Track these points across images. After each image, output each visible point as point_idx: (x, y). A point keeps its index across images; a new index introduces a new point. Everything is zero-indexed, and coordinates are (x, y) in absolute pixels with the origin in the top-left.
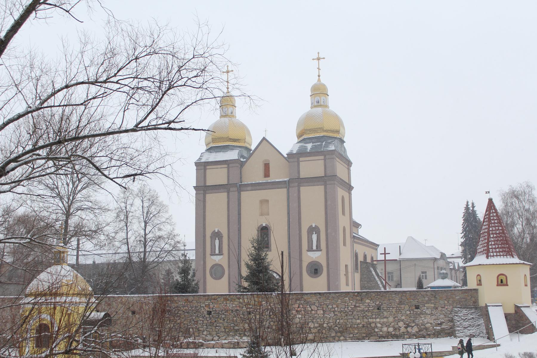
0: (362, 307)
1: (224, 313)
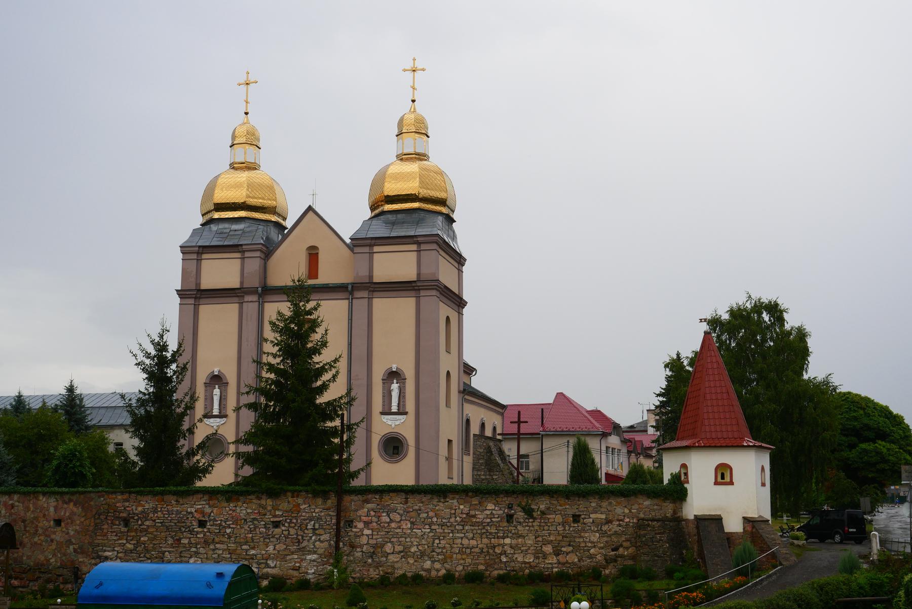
0: (480, 516)
1: (230, 524)
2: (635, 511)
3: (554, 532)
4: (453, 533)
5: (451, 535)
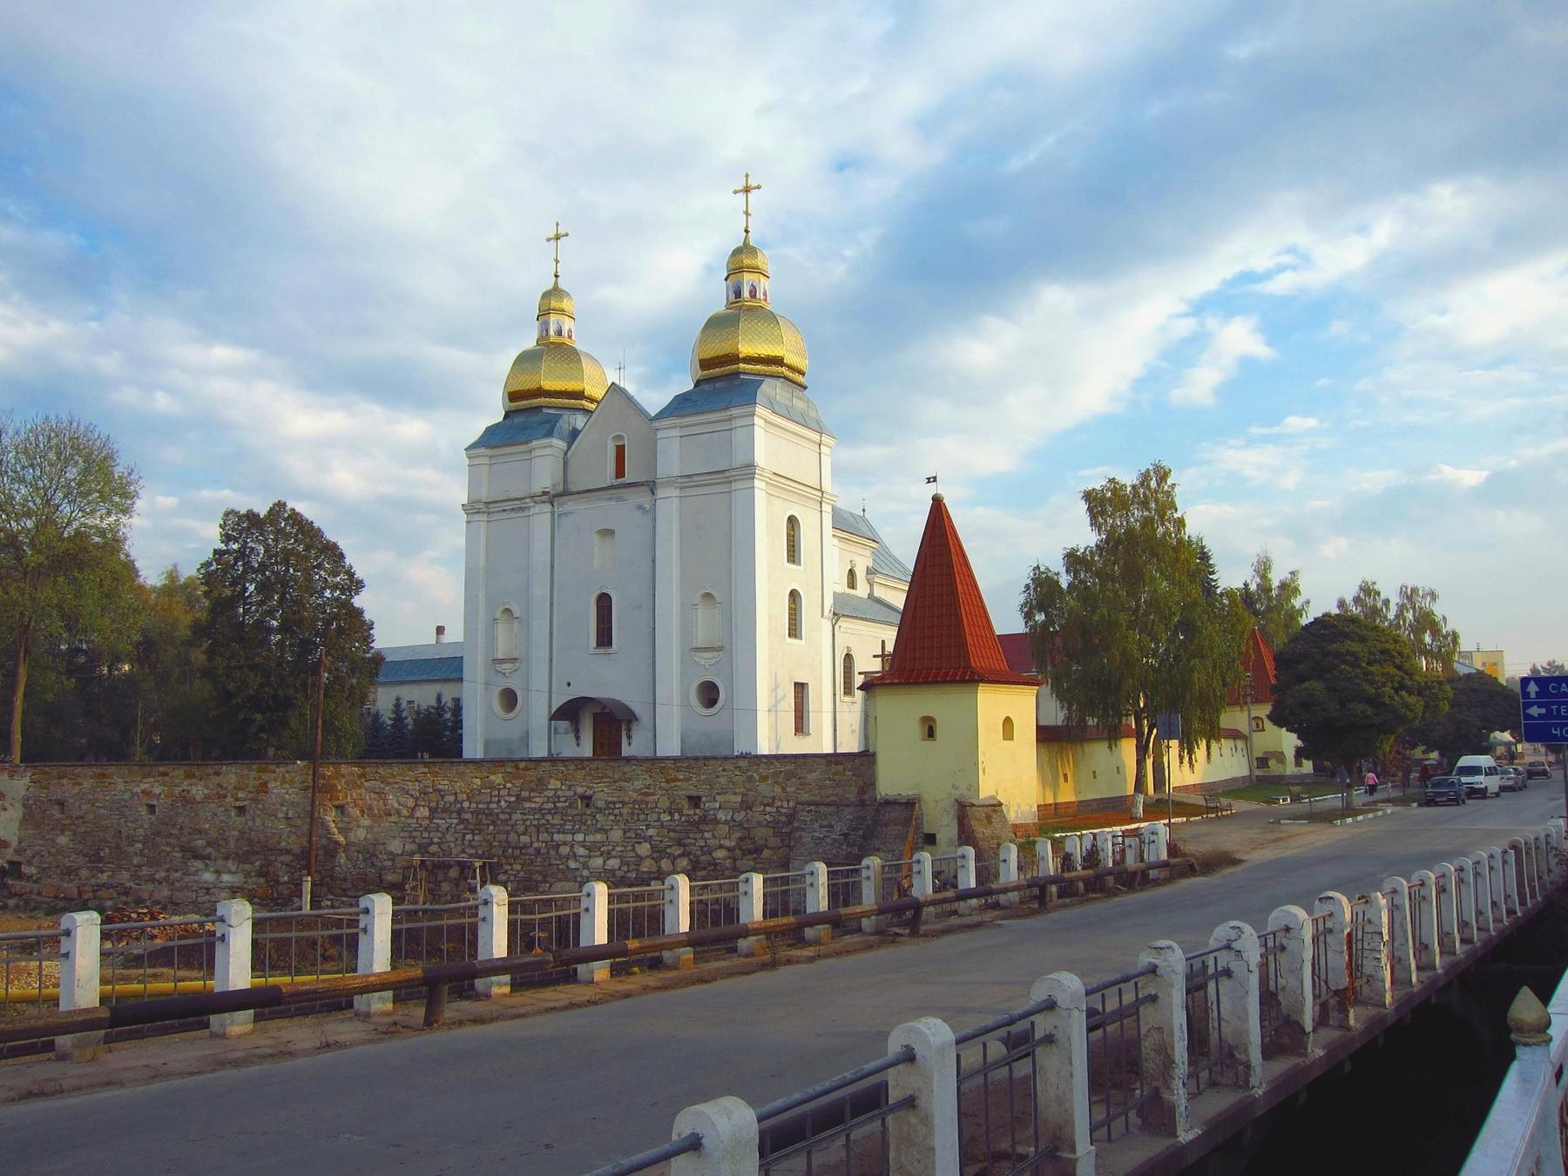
0: (537, 800)
3: (656, 823)
5: (491, 828)
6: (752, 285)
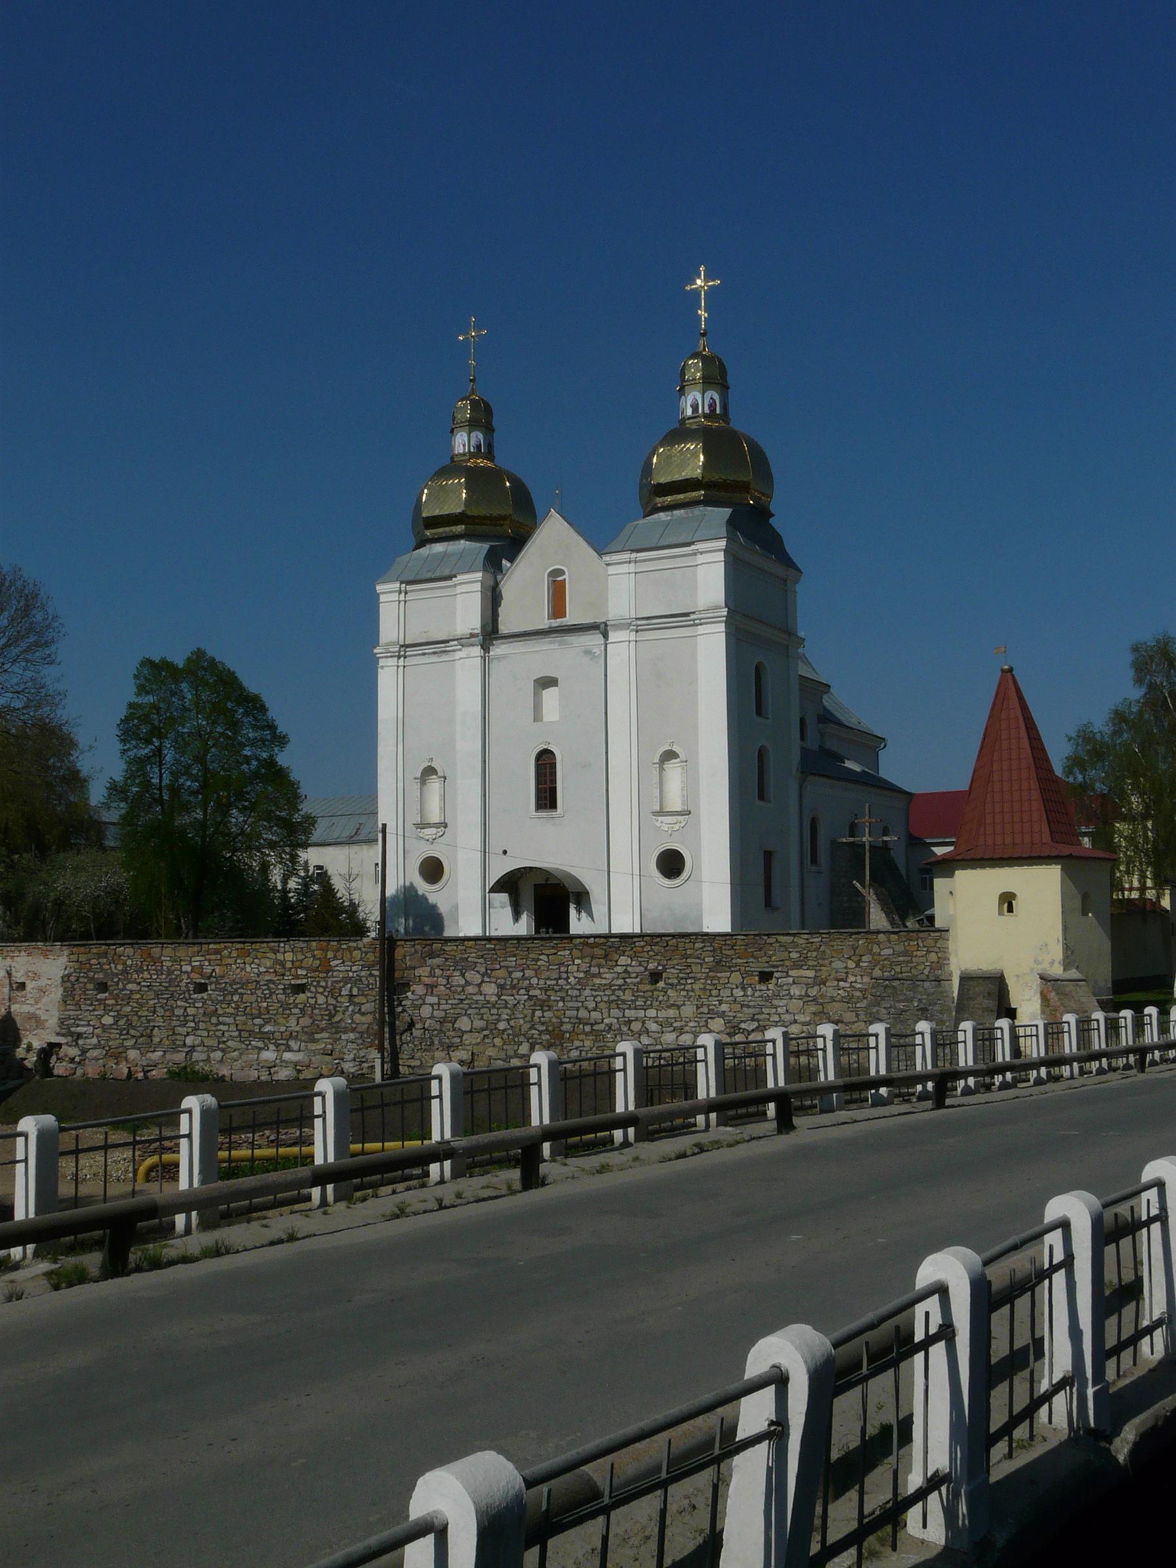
2: (866, 964)
3: (728, 999)
4: (564, 1001)
5: (561, 1004)
6: (712, 398)
